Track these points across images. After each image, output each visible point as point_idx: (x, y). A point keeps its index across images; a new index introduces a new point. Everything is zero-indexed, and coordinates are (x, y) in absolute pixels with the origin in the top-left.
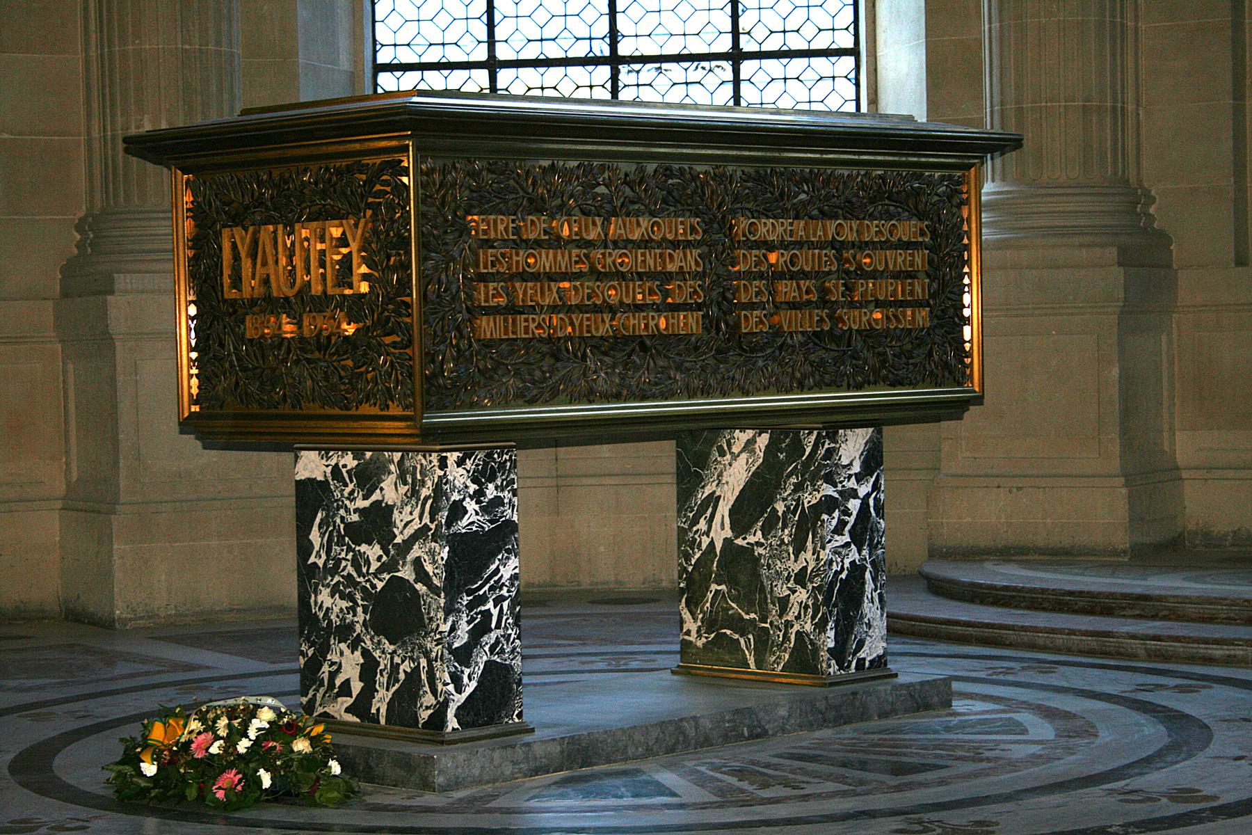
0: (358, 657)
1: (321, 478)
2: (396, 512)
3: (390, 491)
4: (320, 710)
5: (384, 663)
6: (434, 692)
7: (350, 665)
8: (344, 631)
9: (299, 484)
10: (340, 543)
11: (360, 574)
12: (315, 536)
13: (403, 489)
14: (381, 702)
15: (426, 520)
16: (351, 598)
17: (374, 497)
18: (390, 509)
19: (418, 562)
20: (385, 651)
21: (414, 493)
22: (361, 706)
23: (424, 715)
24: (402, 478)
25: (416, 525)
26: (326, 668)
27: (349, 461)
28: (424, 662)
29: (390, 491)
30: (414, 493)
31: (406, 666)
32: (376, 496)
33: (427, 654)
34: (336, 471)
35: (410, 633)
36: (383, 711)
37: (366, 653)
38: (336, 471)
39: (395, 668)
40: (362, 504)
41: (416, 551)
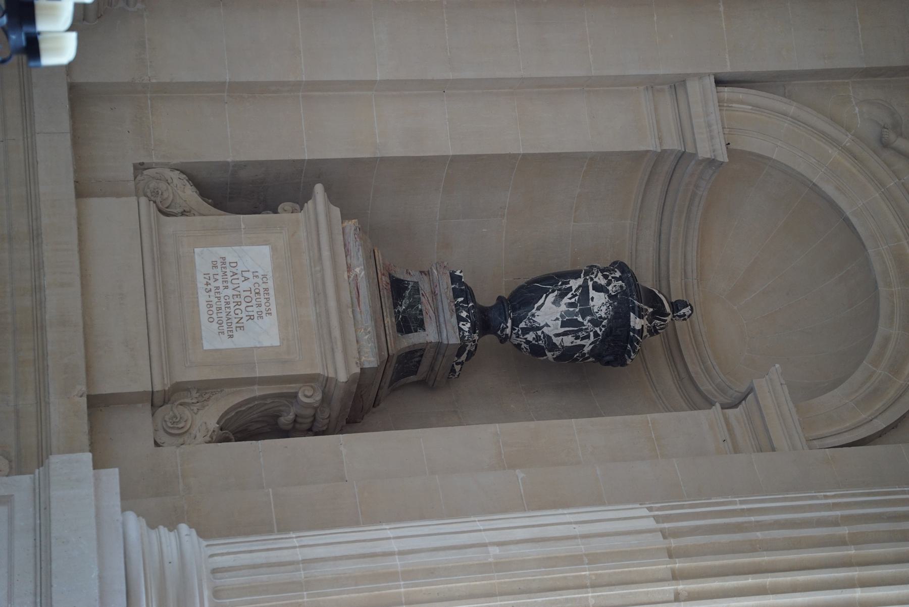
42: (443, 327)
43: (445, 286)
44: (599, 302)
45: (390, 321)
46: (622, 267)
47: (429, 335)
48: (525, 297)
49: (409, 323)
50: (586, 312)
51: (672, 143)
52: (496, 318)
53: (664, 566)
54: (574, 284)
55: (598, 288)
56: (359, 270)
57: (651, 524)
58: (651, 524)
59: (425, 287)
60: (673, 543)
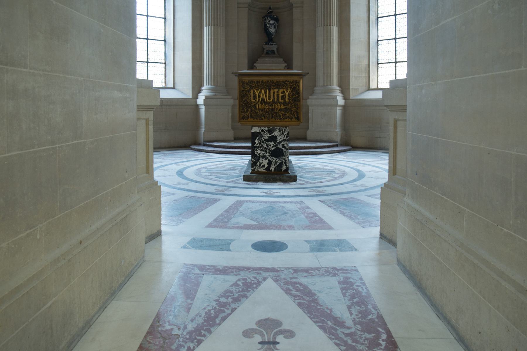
0: (267, 161)
1: (258, 131)
2: (278, 137)
3: (276, 133)
4: (256, 170)
5: (274, 161)
6: (286, 165)
7: (265, 162)
8: (263, 157)
9: (252, 133)
10: (263, 142)
11: (268, 146)
12: (256, 141)
13: (280, 133)
14: (273, 168)
15: (285, 138)
16: (265, 151)
17: (273, 134)
18: (276, 136)
19: (283, 145)
20: (274, 160)
21: (283, 133)
22: (268, 169)
23: (283, 169)
24: (280, 131)
25: (283, 139)
26: (258, 164)
27: (266, 129)
28: (284, 161)
29: (276, 133)
30: (283, 133)
31: (280, 162)
32: (273, 134)
33: (285, 159)
34: (263, 131)
35: (280, 156)
36: (273, 169)
37: (269, 160)
38: (263, 131)
39: (276, 162)
40: (269, 135)
41: (282, 143)
42: (274, 47)
43: (267, 46)
44: (271, 22)
45: (274, 55)
46: (265, 16)
47: (275, 49)
48: (268, 34)
49: (273, 52)
50: (273, 24)
51: (247, 6)
52: (270, 38)
53: (329, 27)
54: (268, 25)
55: (269, 22)
56: (267, 59)
57: (322, 27)
58: (322, 27)
59: (267, 49)
60: (325, 25)
